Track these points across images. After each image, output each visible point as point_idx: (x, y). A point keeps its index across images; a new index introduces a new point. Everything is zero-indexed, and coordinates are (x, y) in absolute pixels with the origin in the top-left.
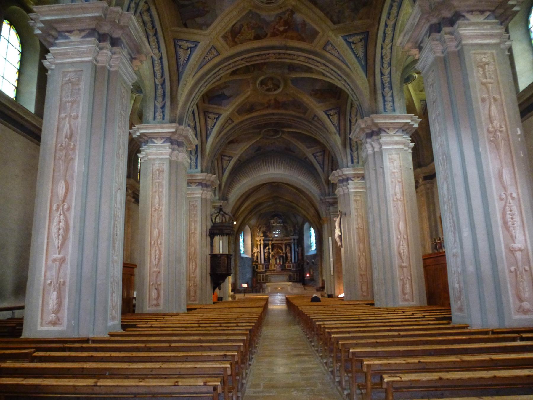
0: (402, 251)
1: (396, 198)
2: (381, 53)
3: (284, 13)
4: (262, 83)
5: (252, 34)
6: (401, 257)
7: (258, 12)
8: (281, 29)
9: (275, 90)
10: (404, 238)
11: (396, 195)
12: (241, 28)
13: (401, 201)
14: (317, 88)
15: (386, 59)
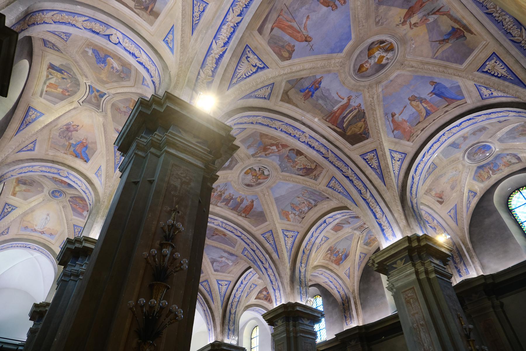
3: (260, 157)
4: (380, 66)
5: (300, 160)
7: (278, 167)
8: (274, 148)
9: (382, 42)
12: (301, 169)
14: (324, 9)
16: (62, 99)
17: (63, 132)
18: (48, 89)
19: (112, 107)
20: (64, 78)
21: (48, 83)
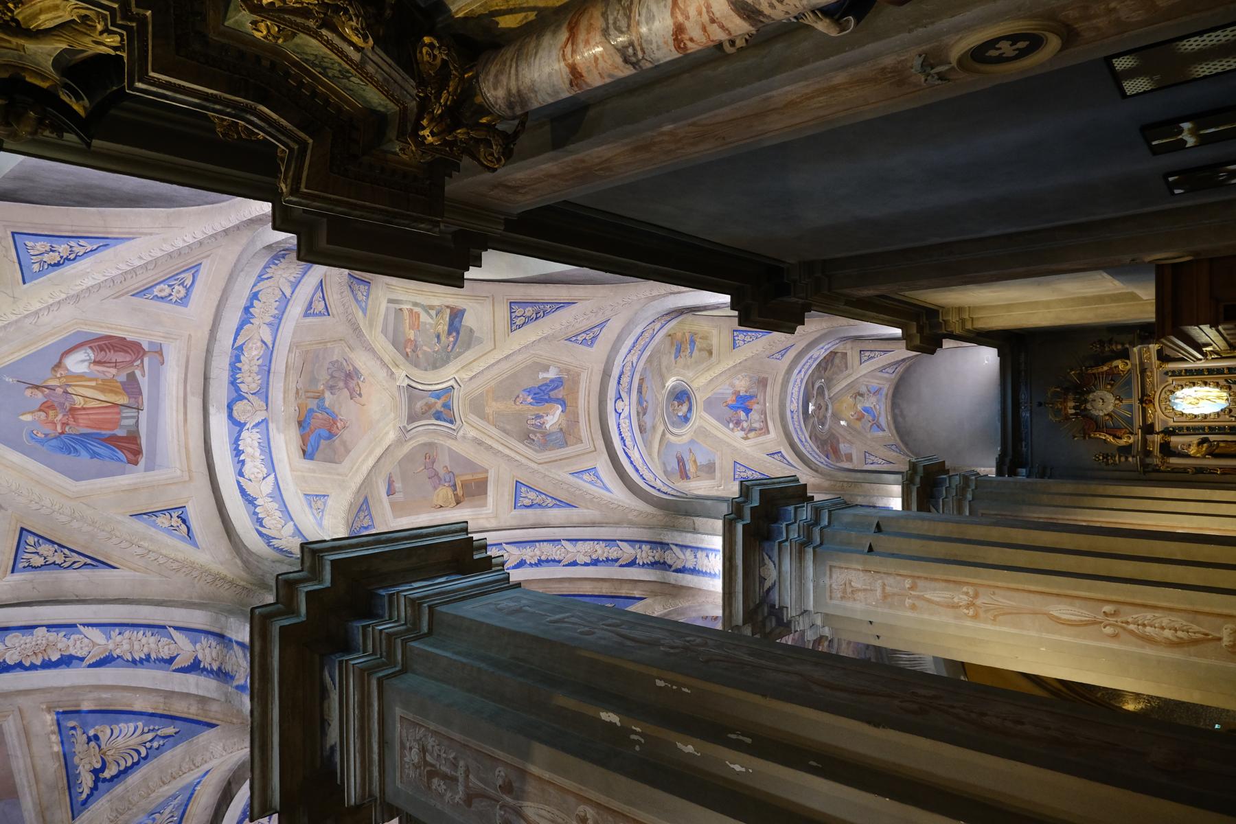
0: (1168, 633)
1: (968, 607)
2: (586, 564)
6: (1195, 642)
10: (1115, 614)
11: (955, 607)
13: (976, 596)
15: (600, 552)
16: (395, 344)
17: (341, 369)
18: (406, 313)
19: (425, 444)
20: (438, 337)
21: (416, 309)
